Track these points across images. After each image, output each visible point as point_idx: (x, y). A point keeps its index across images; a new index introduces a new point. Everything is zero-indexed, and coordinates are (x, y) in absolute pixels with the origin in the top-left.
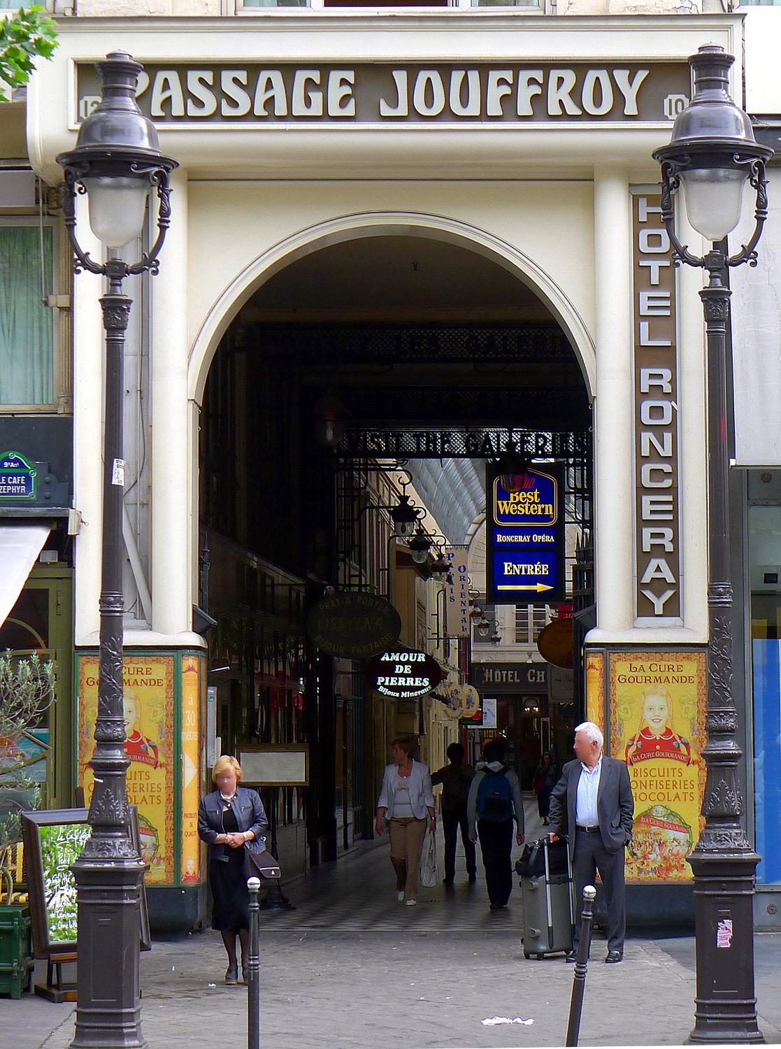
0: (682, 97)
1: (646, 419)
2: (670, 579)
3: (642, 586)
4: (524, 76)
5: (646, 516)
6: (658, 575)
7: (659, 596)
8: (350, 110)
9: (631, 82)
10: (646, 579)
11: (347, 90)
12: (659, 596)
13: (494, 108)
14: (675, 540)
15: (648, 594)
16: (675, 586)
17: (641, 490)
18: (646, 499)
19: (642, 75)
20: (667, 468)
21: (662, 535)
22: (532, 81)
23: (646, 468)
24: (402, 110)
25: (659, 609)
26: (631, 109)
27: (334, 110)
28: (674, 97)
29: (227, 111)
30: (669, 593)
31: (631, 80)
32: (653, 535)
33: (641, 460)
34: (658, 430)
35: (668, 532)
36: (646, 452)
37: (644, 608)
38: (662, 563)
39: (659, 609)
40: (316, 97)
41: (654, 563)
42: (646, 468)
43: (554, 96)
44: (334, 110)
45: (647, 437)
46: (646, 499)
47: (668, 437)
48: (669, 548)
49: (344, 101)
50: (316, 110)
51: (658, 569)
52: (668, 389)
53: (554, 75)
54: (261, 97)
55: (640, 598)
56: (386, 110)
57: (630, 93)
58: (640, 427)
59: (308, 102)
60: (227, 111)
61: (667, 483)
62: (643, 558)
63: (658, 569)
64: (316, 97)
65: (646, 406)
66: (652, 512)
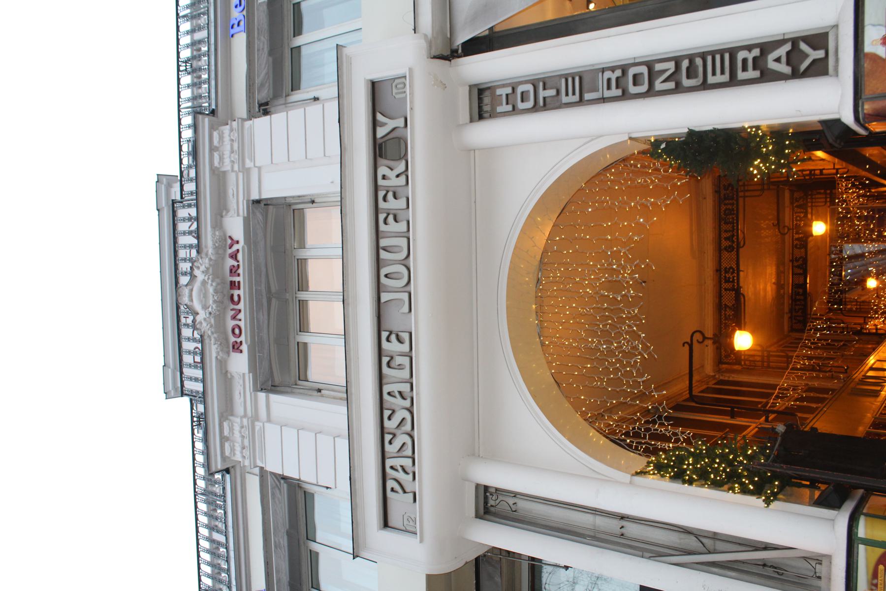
0: (394, 85)
1: (644, 88)
2: (788, 47)
3: (796, 74)
4: (382, 204)
5: (726, 78)
6: (784, 59)
7: (806, 56)
8: (405, 336)
9: (386, 124)
10: (787, 70)
11: (393, 337)
12: (806, 56)
13: (402, 227)
14: (749, 48)
15: (803, 66)
16: (795, 42)
17: (705, 86)
18: (711, 80)
19: (379, 117)
20: (685, 64)
21: (745, 61)
22: (385, 199)
23: (686, 83)
24: (405, 296)
25: (820, 54)
26: (400, 122)
27: (405, 348)
28: (395, 91)
29: (408, 427)
30: (803, 46)
31: (383, 125)
32: (745, 69)
33: (679, 89)
34: (652, 75)
35: (741, 55)
36: (671, 85)
37: (819, 69)
38: (772, 57)
39: (820, 54)
40: (399, 360)
41: (772, 65)
42: (686, 83)
43: (395, 182)
44: (405, 348)
45: (659, 86)
46: (711, 80)
47: (658, 67)
48: (756, 52)
49: (400, 340)
50: (406, 361)
51: (778, 60)
52: (618, 73)
53: (381, 182)
54: (399, 401)
55: (806, 74)
56: (406, 308)
57: (391, 124)
58: (651, 92)
59: (400, 367)
60: (408, 427)
61: (699, 61)
62: (767, 76)
63: (778, 60)
64: (399, 360)
65: (633, 89)
66: (723, 72)
